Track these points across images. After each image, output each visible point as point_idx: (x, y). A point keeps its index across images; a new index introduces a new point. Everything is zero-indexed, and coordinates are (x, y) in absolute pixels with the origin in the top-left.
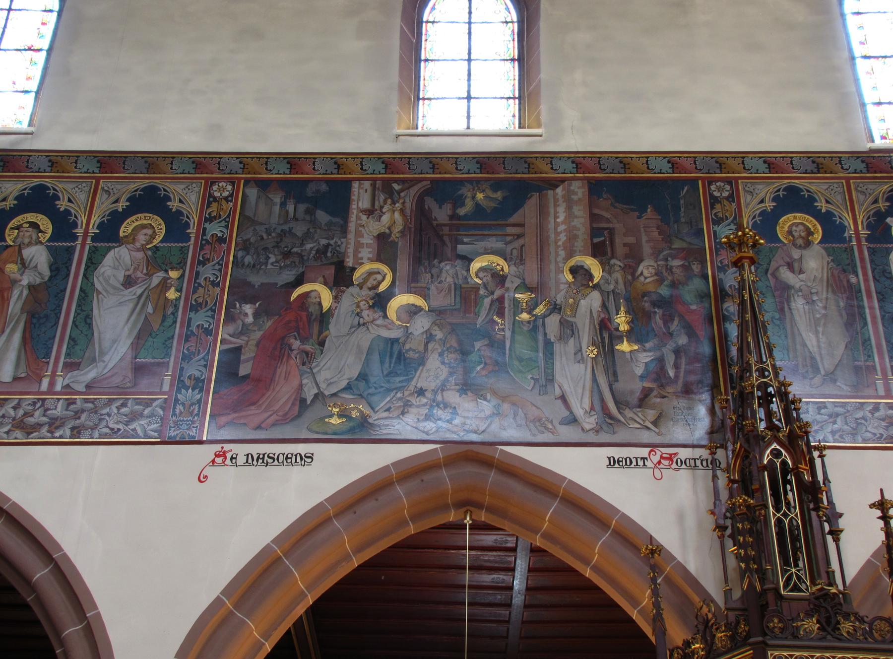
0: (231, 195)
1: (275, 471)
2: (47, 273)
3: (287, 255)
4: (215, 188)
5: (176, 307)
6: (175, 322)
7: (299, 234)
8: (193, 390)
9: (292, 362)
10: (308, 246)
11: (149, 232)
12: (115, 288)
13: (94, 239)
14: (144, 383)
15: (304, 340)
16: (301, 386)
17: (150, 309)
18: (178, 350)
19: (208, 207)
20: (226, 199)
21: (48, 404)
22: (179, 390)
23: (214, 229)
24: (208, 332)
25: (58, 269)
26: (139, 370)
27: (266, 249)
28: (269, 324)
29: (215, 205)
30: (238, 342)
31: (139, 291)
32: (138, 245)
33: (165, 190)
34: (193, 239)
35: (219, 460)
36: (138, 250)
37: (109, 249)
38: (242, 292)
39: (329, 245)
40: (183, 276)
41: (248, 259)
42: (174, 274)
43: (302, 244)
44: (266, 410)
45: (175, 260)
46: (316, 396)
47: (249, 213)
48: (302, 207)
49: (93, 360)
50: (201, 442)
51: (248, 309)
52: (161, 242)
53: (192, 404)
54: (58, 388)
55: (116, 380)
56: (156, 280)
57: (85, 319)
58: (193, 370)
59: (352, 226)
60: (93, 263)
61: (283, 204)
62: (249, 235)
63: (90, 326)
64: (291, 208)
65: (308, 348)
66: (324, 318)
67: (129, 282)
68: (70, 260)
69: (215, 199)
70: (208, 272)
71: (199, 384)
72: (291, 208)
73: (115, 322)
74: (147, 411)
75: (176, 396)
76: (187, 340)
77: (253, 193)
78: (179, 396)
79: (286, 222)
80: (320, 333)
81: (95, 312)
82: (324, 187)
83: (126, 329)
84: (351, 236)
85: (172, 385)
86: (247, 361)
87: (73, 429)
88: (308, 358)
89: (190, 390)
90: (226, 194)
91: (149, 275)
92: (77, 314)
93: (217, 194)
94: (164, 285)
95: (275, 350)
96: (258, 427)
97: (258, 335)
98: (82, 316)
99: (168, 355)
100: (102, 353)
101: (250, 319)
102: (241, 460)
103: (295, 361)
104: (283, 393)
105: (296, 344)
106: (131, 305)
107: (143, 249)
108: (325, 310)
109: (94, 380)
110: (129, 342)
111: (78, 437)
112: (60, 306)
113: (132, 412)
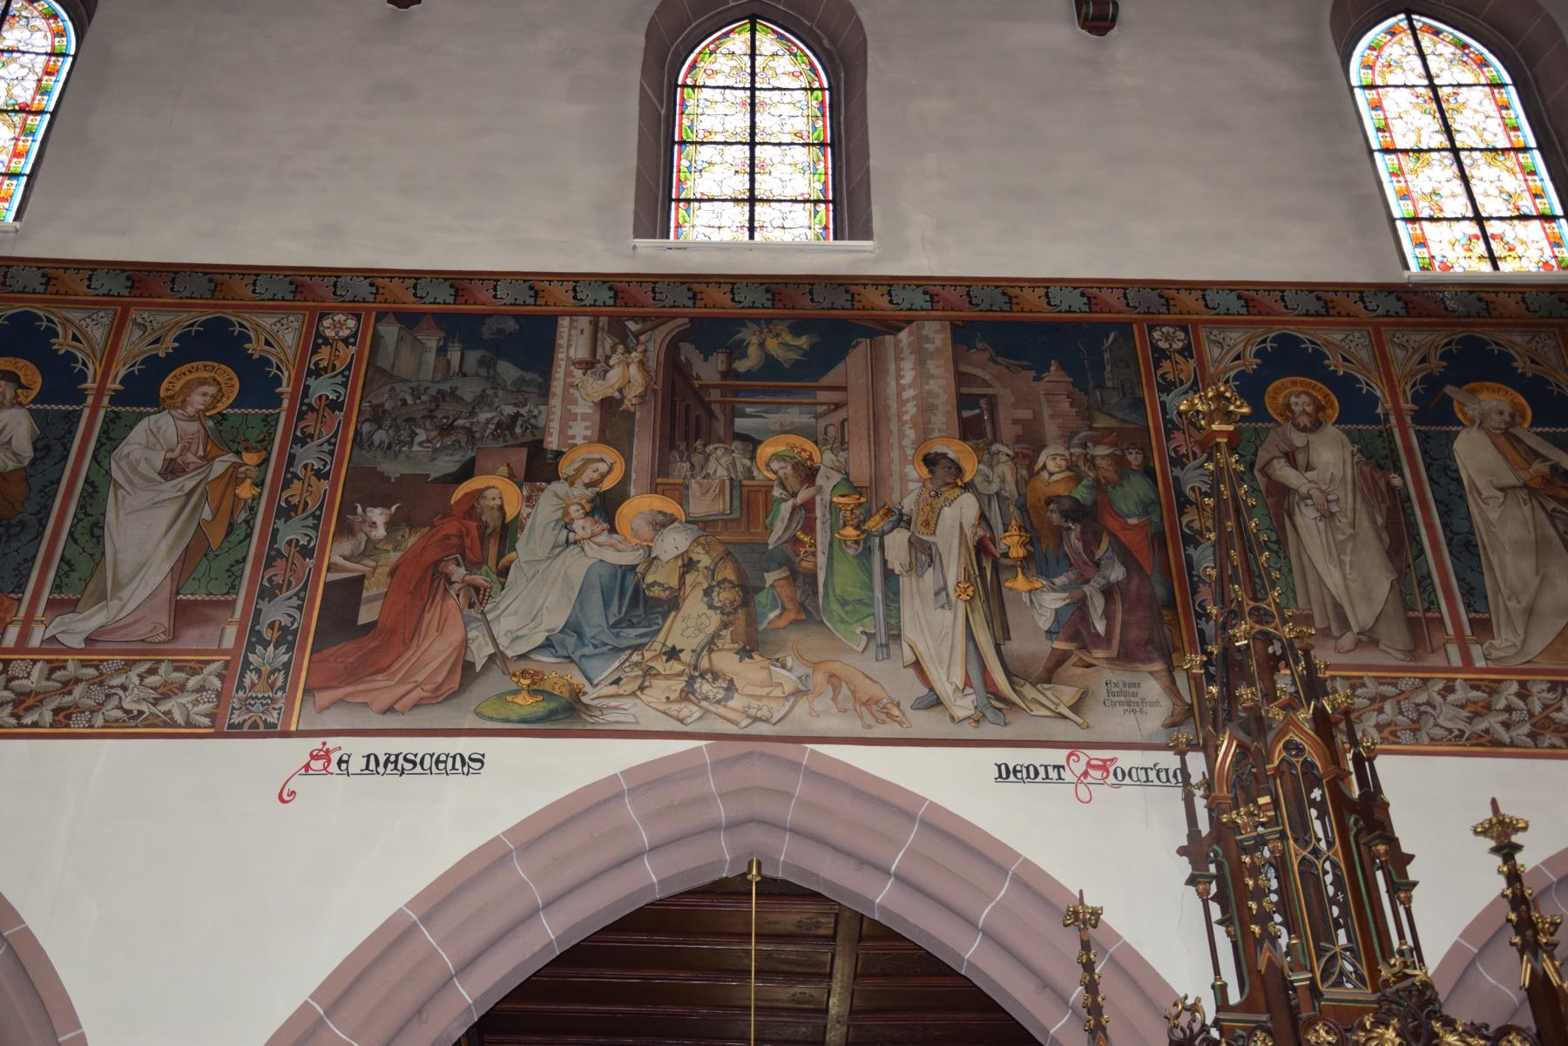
0: (355, 335)
1: (414, 783)
2: (28, 453)
3: (447, 429)
4: (327, 323)
5: (252, 510)
6: (249, 535)
7: (468, 397)
8: (276, 648)
9: (451, 603)
10: (483, 416)
11: (212, 390)
12: (146, 478)
13: (113, 401)
14: (192, 638)
15: (472, 566)
16: (465, 643)
17: (207, 514)
18: (252, 582)
19: (314, 352)
20: (345, 341)
21: (15, 669)
22: (251, 648)
23: (323, 388)
24: (306, 552)
25: (47, 448)
26: (183, 614)
27: (410, 420)
28: (412, 540)
29: (325, 351)
30: (358, 568)
31: (189, 485)
32: (190, 410)
33: (241, 325)
34: (285, 403)
35: (317, 765)
36: (191, 419)
37: (141, 416)
38: (367, 487)
39: (518, 415)
40: (266, 460)
41: (380, 436)
42: (251, 459)
43: (473, 414)
44: (402, 681)
45: (253, 435)
46: (491, 658)
47: (383, 362)
48: (473, 356)
49: (102, 597)
50: (286, 734)
51: (378, 516)
52: (231, 406)
53: (272, 672)
54: (35, 641)
55: (142, 630)
56: (219, 467)
57: (92, 529)
58: (278, 612)
59: (557, 387)
60: (111, 438)
61: (442, 351)
62: (383, 397)
63: (99, 540)
64: (455, 356)
65: (479, 579)
66: (507, 532)
67: (172, 470)
68: (71, 433)
69: (326, 341)
70: (309, 456)
71: (286, 638)
72: (455, 356)
73: (144, 536)
74: (193, 682)
75: (246, 657)
76: (269, 565)
77: (390, 331)
78: (252, 657)
79: (446, 377)
80: (501, 555)
81: (110, 517)
82: (511, 325)
83: (164, 546)
84: (556, 402)
85: (239, 639)
86: (374, 599)
87: (56, 711)
88: (478, 596)
89: (271, 648)
90: (346, 333)
91: (208, 459)
92: (77, 520)
93: (329, 333)
94: (233, 477)
95: (422, 583)
96: (390, 710)
97: (394, 557)
98: (86, 523)
99: (234, 588)
100: (118, 586)
101: (380, 532)
102: (357, 764)
103: (454, 604)
104: (434, 652)
105: (458, 573)
106: (173, 508)
107: (198, 417)
108: (509, 518)
109: (101, 630)
110: (168, 568)
111: (64, 724)
112: (47, 509)
113: (165, 683)
